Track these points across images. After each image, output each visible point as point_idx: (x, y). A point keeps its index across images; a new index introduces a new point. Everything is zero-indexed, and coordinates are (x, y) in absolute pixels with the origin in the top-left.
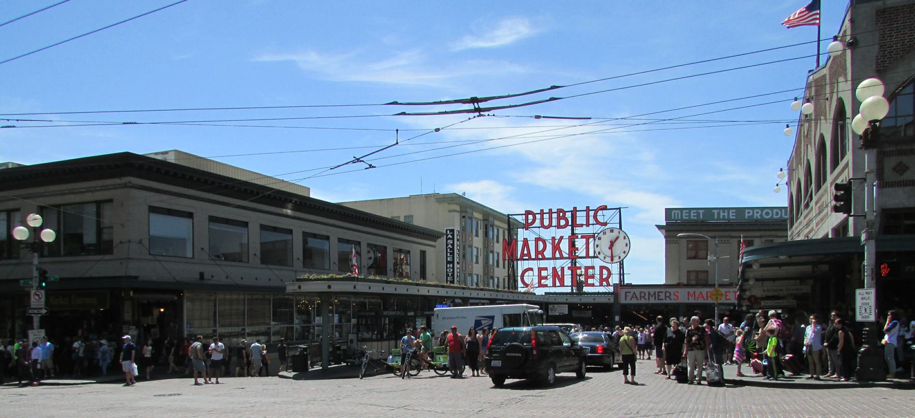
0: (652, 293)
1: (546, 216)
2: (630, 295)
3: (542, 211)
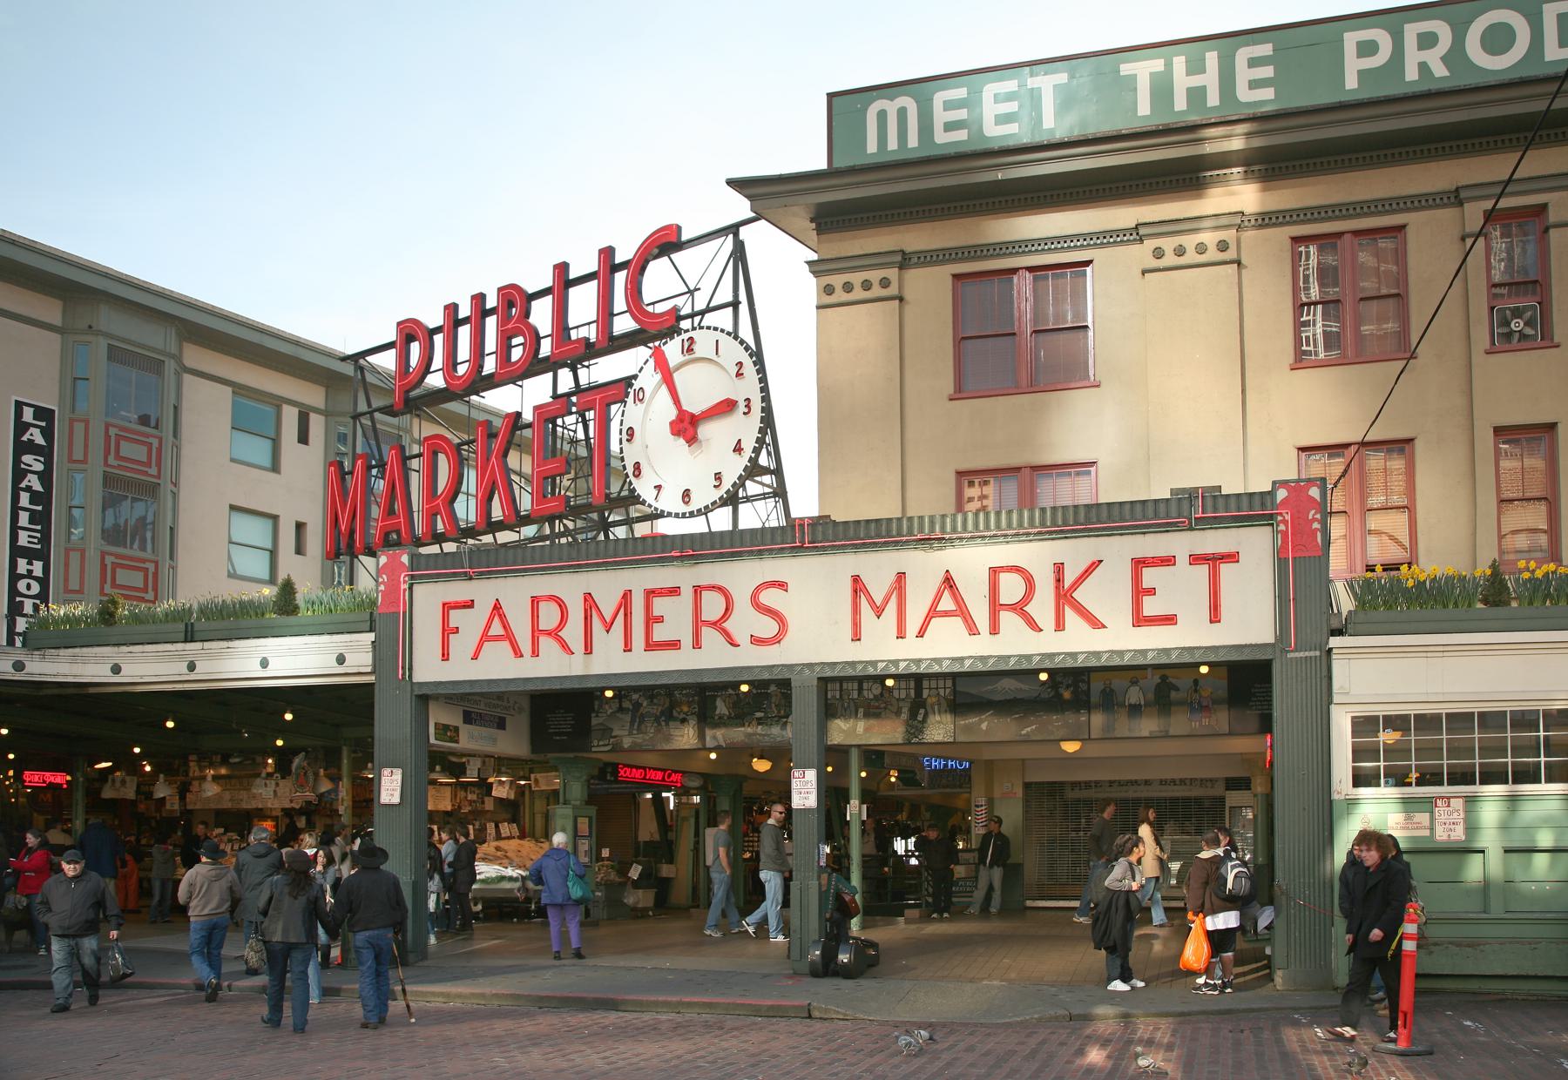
0: (608, 605)
1: (464, 333)
2: (470, 624)
3: (452, 309)
